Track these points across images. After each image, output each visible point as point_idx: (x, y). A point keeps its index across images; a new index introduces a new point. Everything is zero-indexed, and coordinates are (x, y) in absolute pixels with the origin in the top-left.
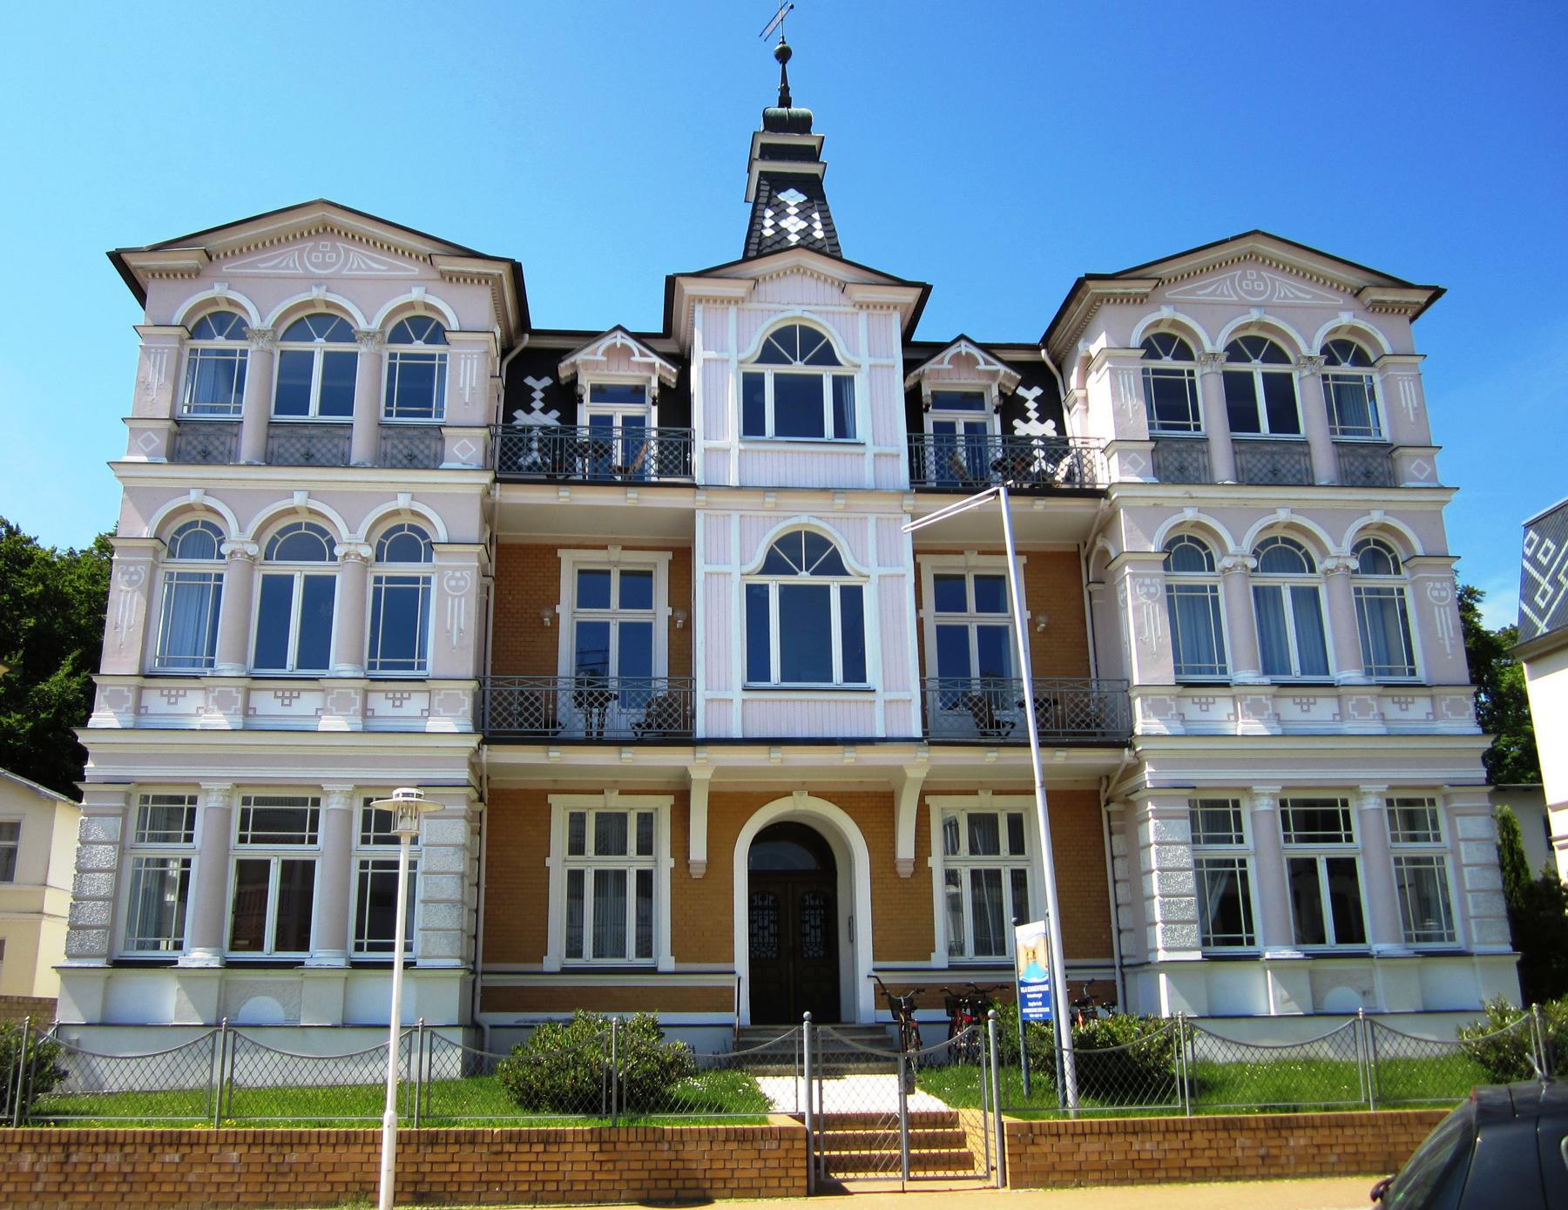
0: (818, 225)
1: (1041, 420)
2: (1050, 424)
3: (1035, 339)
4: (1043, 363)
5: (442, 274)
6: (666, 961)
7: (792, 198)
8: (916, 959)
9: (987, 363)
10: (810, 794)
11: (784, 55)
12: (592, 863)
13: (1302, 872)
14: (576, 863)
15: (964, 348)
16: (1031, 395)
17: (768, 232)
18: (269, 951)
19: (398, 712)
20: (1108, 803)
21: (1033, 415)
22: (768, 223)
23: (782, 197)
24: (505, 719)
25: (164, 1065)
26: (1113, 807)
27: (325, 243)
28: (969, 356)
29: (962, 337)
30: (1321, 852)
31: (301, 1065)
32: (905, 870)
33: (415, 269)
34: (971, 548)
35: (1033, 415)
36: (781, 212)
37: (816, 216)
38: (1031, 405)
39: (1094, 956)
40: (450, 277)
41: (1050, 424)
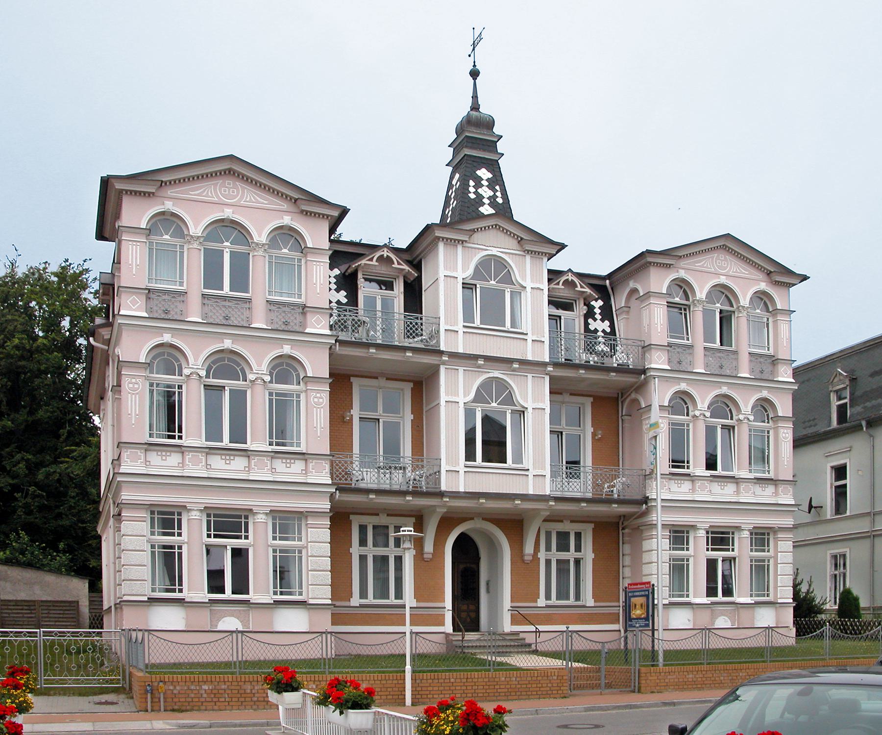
0: (499, 194)
1: (602, 320)
2: (607, 323)
3: (605, 273)
4: (605, 286)
5: (302, 211)
6: (590, 602)
7: (484, 174)
8: (530, 602)
9: (582, 287)
10: (483, 519)
11: (475, 74)
12: (371, 551)
13: (711, 564)
14: (363, 550)
15: (570, 277)
16: (598, 304)
17: (472, 196)
18: (228, 594)
19: (288, 470)
20: (623, 529)
21: (598, 317)
22: (472, 189)
23: (479, 173)
24: (343, 476)
25: (312, 645)
26: (626, 531)
27: (229, 182)
28: (573, 282)
29: (570, 270)
30: (719, 555)
31: (177, 647)
32: (528, 558)
33: (285, 206)
34: (566, 391)
35: (598, 317)
36: (478, 185)
37: (497, 188)
38: (598, 311)
39: (603, 601)
40: (307, 213)
41: (607, 323)
